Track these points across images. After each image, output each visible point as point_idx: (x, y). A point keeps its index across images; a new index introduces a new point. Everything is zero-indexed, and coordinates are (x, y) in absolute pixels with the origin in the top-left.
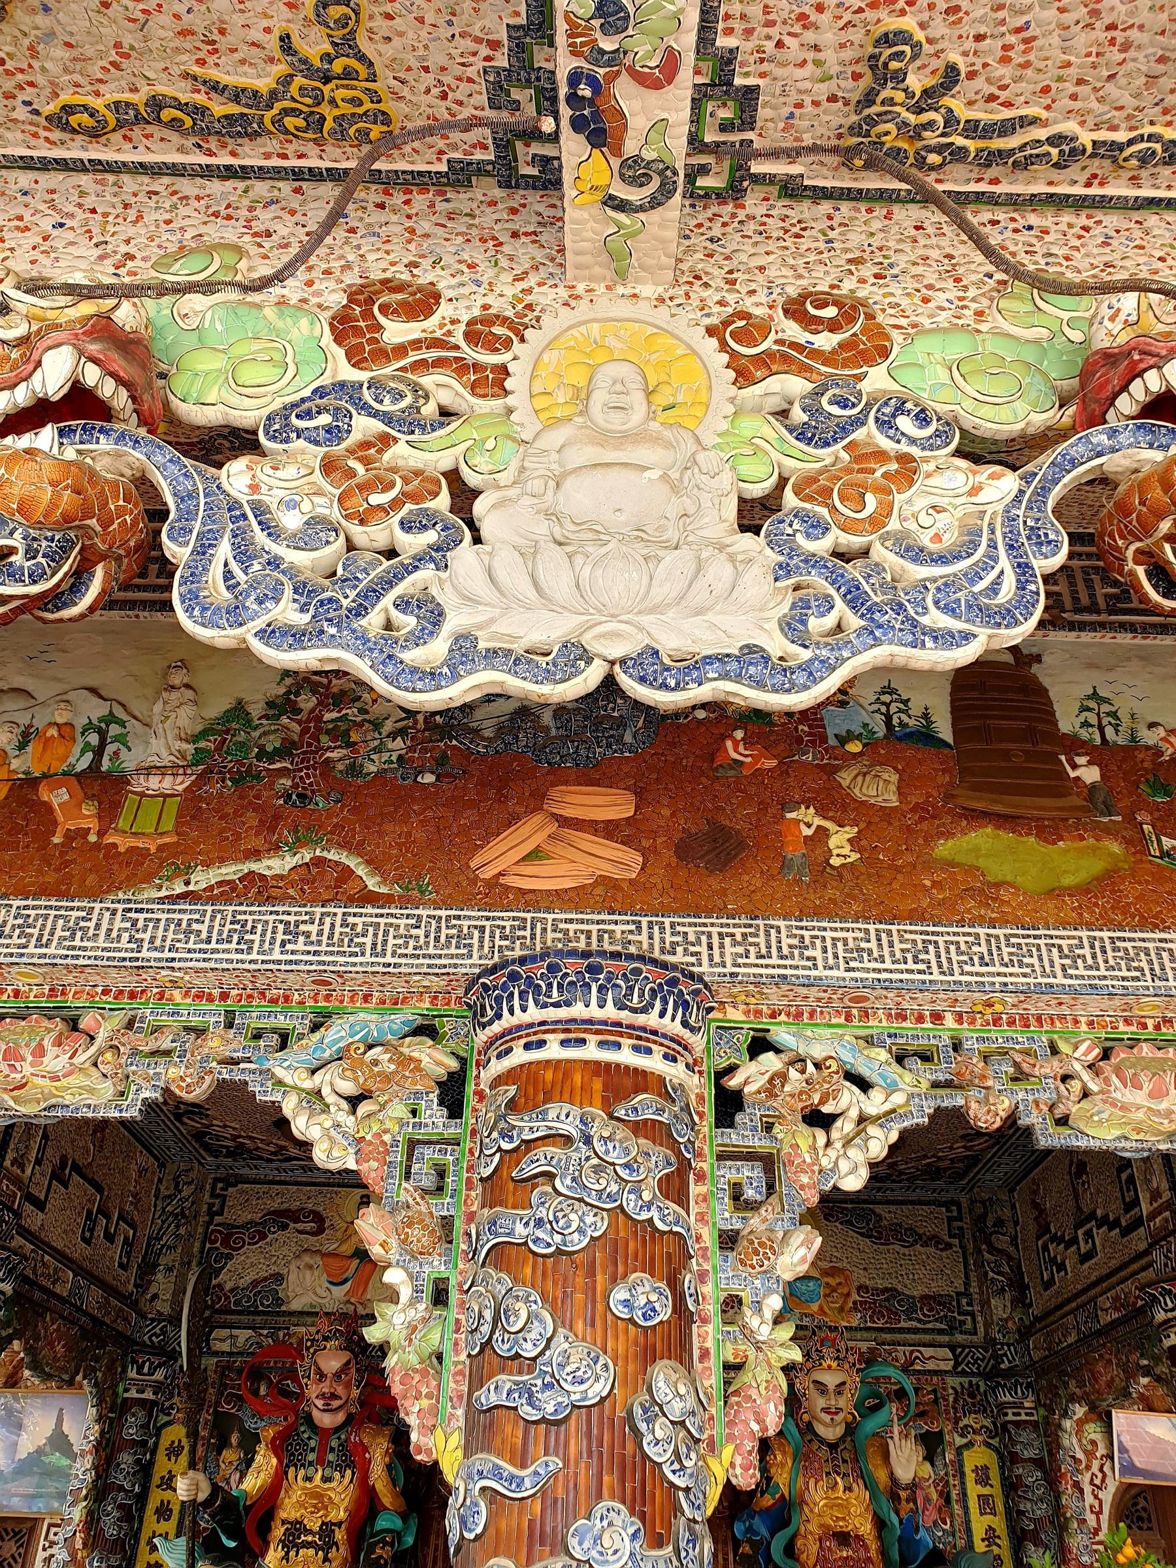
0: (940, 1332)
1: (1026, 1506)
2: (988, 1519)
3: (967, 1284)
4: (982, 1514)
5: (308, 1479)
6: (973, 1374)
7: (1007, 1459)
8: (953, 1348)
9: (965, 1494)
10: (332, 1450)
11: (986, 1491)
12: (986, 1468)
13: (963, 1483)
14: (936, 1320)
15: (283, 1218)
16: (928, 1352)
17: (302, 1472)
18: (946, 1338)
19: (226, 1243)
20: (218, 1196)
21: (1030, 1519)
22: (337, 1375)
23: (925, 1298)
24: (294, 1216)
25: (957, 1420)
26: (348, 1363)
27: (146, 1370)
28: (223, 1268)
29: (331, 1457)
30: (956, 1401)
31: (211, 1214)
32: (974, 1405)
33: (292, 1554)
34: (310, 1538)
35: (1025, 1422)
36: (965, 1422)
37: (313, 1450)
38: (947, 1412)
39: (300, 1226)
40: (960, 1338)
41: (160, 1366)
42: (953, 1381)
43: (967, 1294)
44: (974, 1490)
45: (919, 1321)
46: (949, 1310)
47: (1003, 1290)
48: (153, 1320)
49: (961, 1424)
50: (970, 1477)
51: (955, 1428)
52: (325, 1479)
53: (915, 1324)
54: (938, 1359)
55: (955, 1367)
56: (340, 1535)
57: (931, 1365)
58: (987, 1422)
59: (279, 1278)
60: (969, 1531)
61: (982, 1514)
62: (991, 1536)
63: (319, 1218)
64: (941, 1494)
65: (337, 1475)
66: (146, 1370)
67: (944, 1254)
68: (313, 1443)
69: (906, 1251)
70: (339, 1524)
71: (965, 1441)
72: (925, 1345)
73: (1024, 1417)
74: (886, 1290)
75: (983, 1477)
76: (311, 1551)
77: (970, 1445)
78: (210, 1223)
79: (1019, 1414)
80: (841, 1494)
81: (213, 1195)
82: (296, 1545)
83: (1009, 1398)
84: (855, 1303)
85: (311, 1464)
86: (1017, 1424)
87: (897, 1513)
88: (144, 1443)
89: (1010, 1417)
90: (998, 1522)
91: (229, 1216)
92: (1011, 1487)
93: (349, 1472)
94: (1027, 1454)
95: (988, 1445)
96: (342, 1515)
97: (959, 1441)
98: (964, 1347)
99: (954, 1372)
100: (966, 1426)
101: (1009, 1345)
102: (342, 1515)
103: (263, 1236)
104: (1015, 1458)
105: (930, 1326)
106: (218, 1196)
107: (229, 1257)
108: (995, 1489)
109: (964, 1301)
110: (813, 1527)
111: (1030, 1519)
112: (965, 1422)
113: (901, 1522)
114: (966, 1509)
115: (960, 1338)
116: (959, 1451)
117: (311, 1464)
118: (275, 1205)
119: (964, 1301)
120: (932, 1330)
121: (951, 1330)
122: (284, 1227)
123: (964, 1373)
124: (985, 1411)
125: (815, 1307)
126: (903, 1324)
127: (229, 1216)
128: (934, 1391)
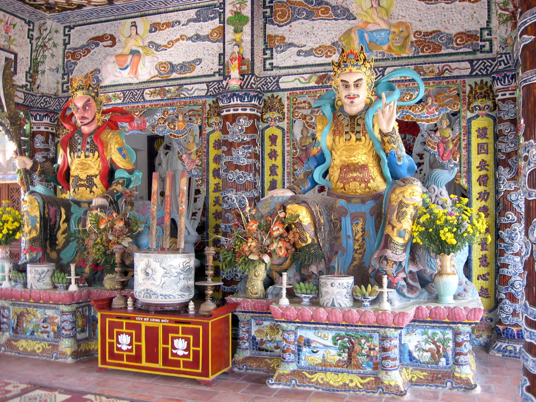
0: (466, 53)
1: (502, 146)
2: (483, 156)
3: (488, 22)
4: (478, 153)
5: (79, 157)
6: (483, 75)
7: (497, 121)
8: (471, 61)
9: (469, 144)
10: (88, 143)
11: (484, 141)
12: (485, 129)
13: (469, 139)
14: (465, 47)
15: (98, 40)
16: (454, 65)
17: (76, 154)
18: (471, 57)
19: (73, 58)
20: (67, 35)
21: (504, 153)
22: (84, 107)
23: (460, 35)
24: (101, 38)
25: (469, 104)
26: (89, 100)
27: (38, 118)
28: (73, 70)
29: (88, 146)
30: (471, 92)
31: (65, 45)
32: (481, 94)
33: (76, 190)
34: (82, 183)
35: (508, 99)
36: (475, 104)
37: (79, 144)
38: (464, 99)
39: (105, 43)
40: (479, 55)
41: (45, 116)
42: (470, 81)
43: (488, 28)
44: (475, 141)
45: (453, 48)
46: (475, 39)
47: (507, 20)
48: (40, 96)
49: (472, 106)
50: (474, 134)
51: (468, 108)
52: (86, 157)
53: (451, 51)
54: (464, 68)
55: (471, 72)
56: (97, 181)
57: (456, 73)
58: (490, 103)
59: (98, 70)
60: (469, 163)
61: (478, 153)
62: (483, 165)
63: (113, 38)
64: (455, 145)
65: (91, 154)
66: (38, 118)
67: (475, 5)
68: (79, 141)
69: (449, 6)
70: (96, 176)
71: (473, 115)
72: (452, 62)
73: (508, 96)
74: (434, 32)
75: (482, 133)
76: (84, 188)
77: (477, 116)
78: (65, 49)
79: (505, 95)
80: (354, 143)
81: (65, 35)
82: (77, 186)
83: (500, 86)
84: (412, 42)
85: (79, 150)
86: (503, 101)
87: (384, 151)
88: (48, 150)
89: (500, 97)
90: (489, 158)
91: (72, 45)
92: (497, 137)
93: (97, 154)
94: (506, 118)
95: (488, 115)
96: (97, 173)
97: (469, 115)
98: (478, 60)
99: (470, 76)
100: (475, 107)
101: (505, 54)
102: (97, 173)
103: (89, 51)
104: (501, 121)
105: (461, 51)
106: (67, 35)
107: (75, 64)
108: (490, 140)
109: (486, 32)
110: (337, 162)
111: (504, 153)
112: (475, 104)
113: (387, 156)
114: (469, 152)
115: (479, 55)
116: (469, 121)
117: (79, 150)
118: (92, 35)
119: (486, 32)
120: (462, 53)
121: (474, 52)
122: (97, 45)
123: (477, 75)
124: (489, 96)
125: (385, 47)
126: (443, 52)
127: (72, 45)
128: (457, 89)
